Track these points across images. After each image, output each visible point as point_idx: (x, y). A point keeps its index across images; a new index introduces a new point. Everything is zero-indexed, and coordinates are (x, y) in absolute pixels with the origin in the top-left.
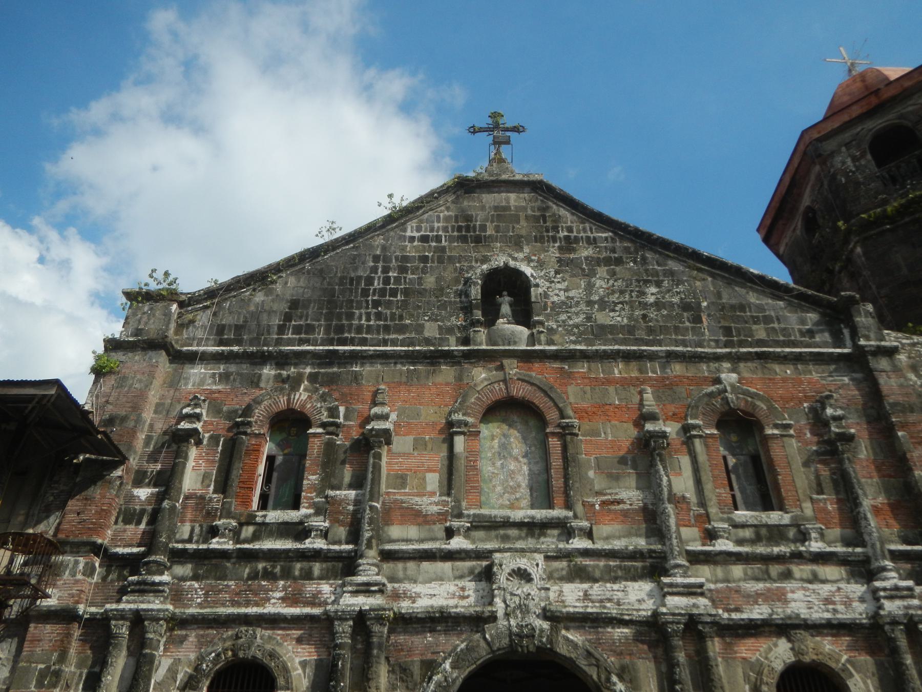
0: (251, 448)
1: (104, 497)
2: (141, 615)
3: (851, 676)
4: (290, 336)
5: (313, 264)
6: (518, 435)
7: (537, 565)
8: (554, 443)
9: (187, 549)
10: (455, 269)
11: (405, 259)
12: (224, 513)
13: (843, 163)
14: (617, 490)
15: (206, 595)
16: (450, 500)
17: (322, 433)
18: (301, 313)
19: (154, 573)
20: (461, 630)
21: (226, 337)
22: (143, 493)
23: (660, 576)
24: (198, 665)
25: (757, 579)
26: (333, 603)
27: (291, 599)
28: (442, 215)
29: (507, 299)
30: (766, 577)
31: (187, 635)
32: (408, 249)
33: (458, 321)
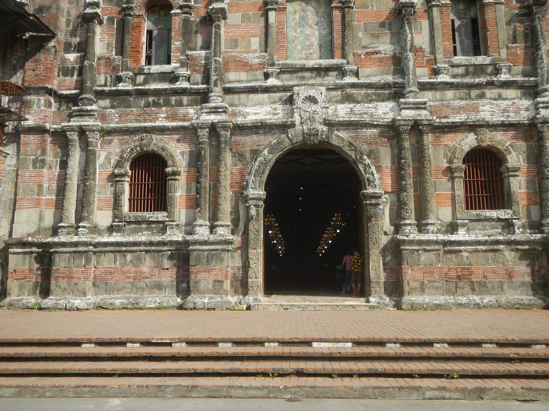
0: (135, 25)
1: (46, 59)
3: (510, 153)
6: (312, 9)
7: (321, 93)
8: (337, 14)
12: (124, 68)
15: (120, 116)
16: (266, 55)
17: (181, 13)
19: (86, 105)
20: (274, 133)
22: (72, 57)
23: (399, 98)
24: (122, 155)
25: (462, 99)
26: (197, 118)
27: (172, 117)
31: (112, 139)
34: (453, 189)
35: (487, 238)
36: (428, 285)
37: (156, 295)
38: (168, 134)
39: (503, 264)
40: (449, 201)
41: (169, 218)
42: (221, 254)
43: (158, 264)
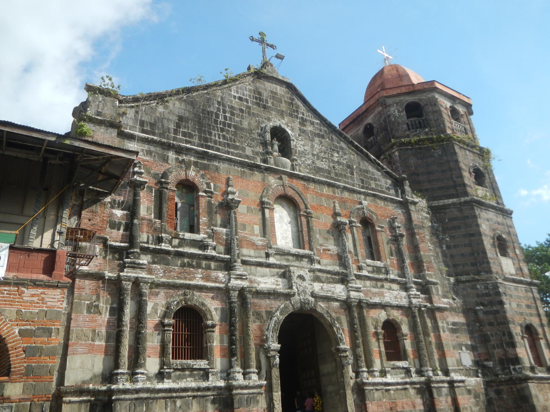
0: (170, 197)
2: (139, 280)
3: (402, 324)
4: (180, 137)
10: (256, 120)
11: (232, 107)
13: (394, 112)
14: (327, 245)
15: (164, 272)
21: (145, 128)
25: (374, 287)
27: (207, 278)
29: (277, 142)
30: (376, 287)
32: (234, 103)
33: (260, 149)
34: (379, 347)
38: (205, 292)
39: (410, 398)
40: (378, 355)
41: (209, 366)
42: (257, 397)
43: (203, 408)
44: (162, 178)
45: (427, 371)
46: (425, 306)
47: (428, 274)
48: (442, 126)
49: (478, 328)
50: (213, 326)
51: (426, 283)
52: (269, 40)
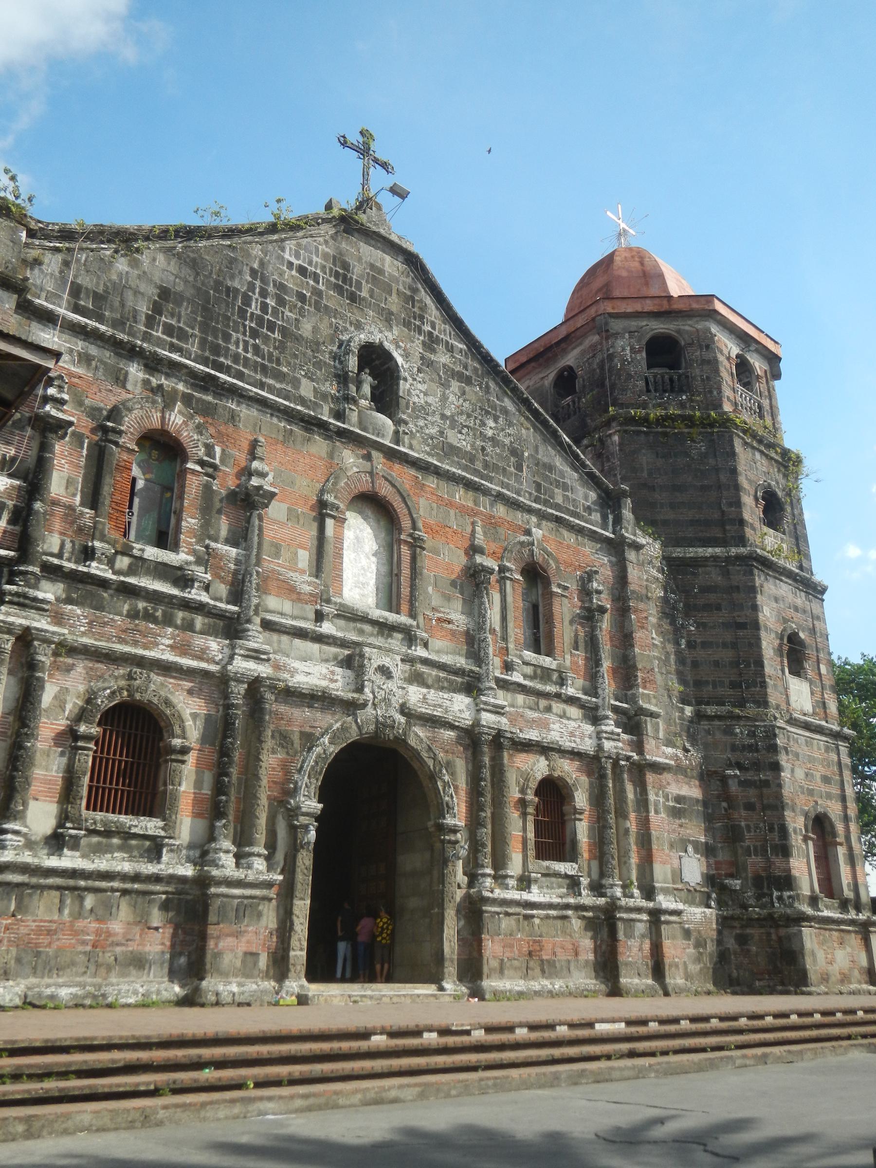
0: (122, 464)
2: (31, 634)
3: (577, 790)
4: (160, 334)
5: (186, 247)
9: (62, 567)
10: (331, 324)
11: (281, 287)
13: (623, 350)
15: (90, 623)
18: (172, 309)
21: (82, 303)
25: (531, 708)
27: (182, 649)
28: (320, 247)
29: (370, 379)
30: (535, 708)
31: (74, 664)
32: (286, 277)
33: (331, 388)
34: (524, 829)
35: (559, 900)
36: (508, 965)
37: (132, 979)
38: (175, 678)
39: (571, 936)
40: (520, 846)
42: (259, 904)
44: (108, 418)
45: (612, 886)
46: (628, 758)
47: (643, 694)
48: (715, 393)
49: (723, 812)
50: (185, 751)
51: (636, 711)
52: (379, 149)
